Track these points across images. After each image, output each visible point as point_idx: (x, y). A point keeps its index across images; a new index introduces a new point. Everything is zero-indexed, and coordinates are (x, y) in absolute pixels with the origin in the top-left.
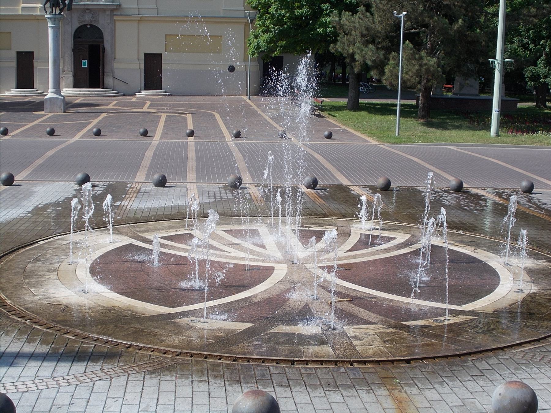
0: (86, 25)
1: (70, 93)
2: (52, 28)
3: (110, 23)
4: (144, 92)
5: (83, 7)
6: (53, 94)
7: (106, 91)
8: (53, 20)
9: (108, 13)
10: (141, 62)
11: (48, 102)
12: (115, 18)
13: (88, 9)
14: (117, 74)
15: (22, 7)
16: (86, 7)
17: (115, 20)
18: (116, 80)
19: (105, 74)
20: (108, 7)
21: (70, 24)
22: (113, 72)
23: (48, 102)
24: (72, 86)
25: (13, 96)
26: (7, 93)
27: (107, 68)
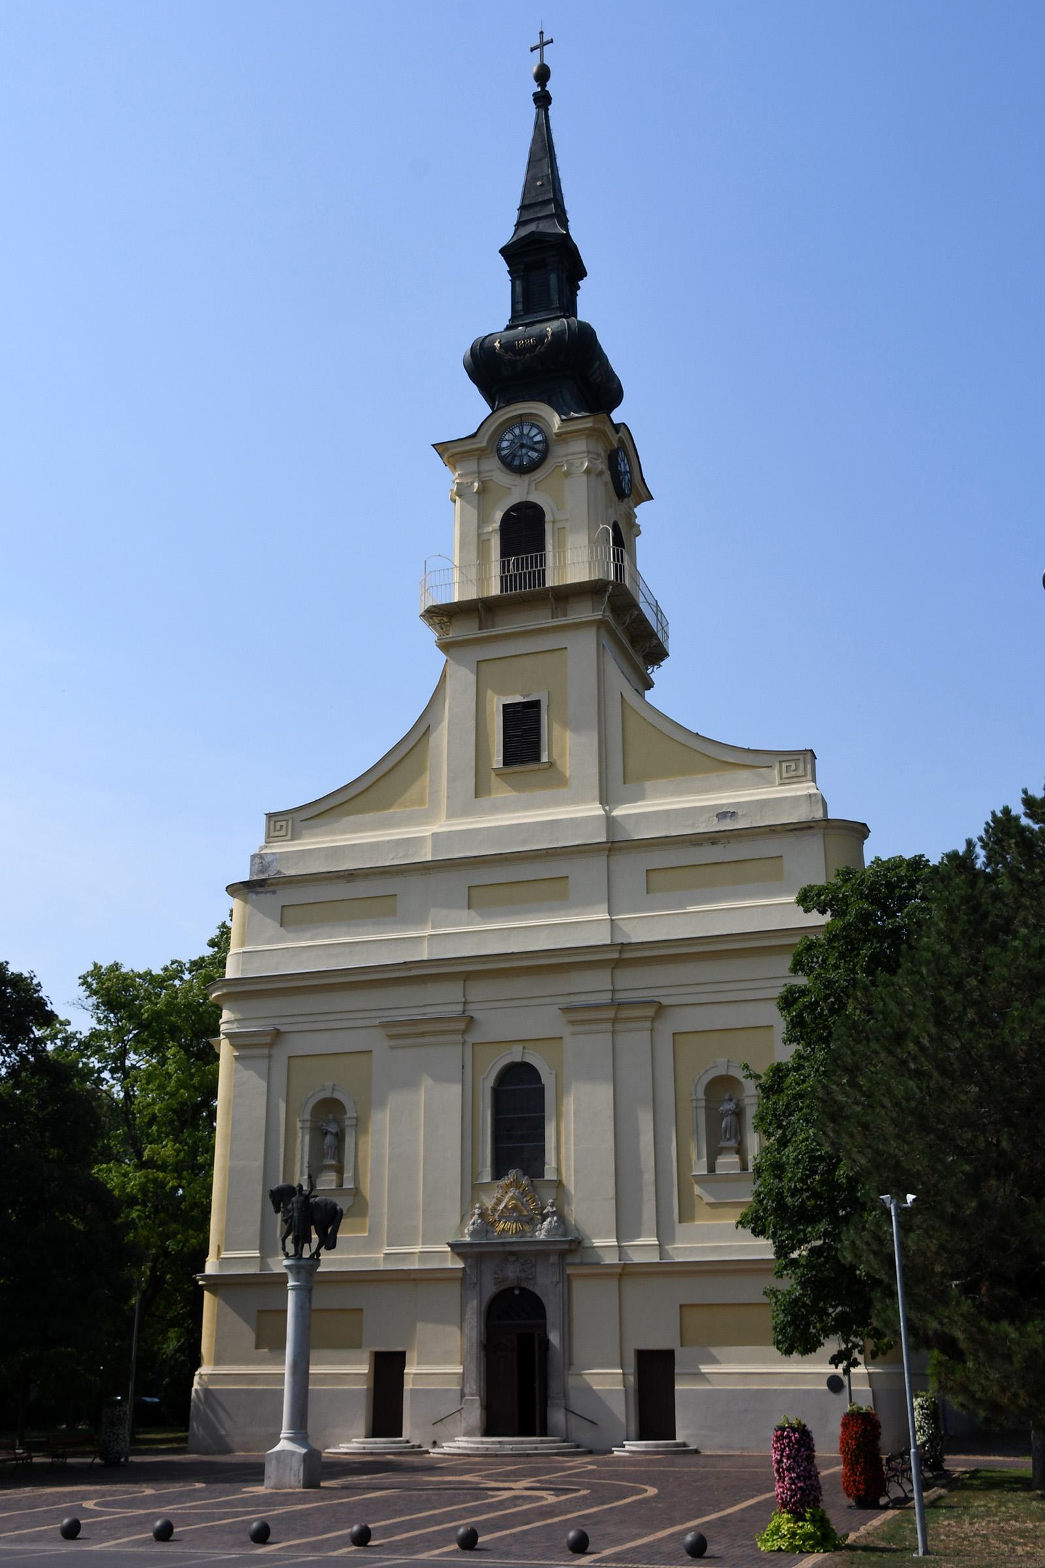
0: (511, 1289)
1: (459, 1448)
2: (294, 1288)
3: (558, 1283)
5: (501, 1249)
7: (542, 1442)
9: (553, 1259)
10: (627, 1371)
11: (274, 1462)
12: (570, 1270)
13: (513, 1253)
14: (576, 1403)
15: (386, 1254)
16: (508, 1248)
17: (569, 1276)
18: (572, 1418)
20: (552, 1247)
22: (566, 1396)
26: (344, 1448)
27: (554, 1387)
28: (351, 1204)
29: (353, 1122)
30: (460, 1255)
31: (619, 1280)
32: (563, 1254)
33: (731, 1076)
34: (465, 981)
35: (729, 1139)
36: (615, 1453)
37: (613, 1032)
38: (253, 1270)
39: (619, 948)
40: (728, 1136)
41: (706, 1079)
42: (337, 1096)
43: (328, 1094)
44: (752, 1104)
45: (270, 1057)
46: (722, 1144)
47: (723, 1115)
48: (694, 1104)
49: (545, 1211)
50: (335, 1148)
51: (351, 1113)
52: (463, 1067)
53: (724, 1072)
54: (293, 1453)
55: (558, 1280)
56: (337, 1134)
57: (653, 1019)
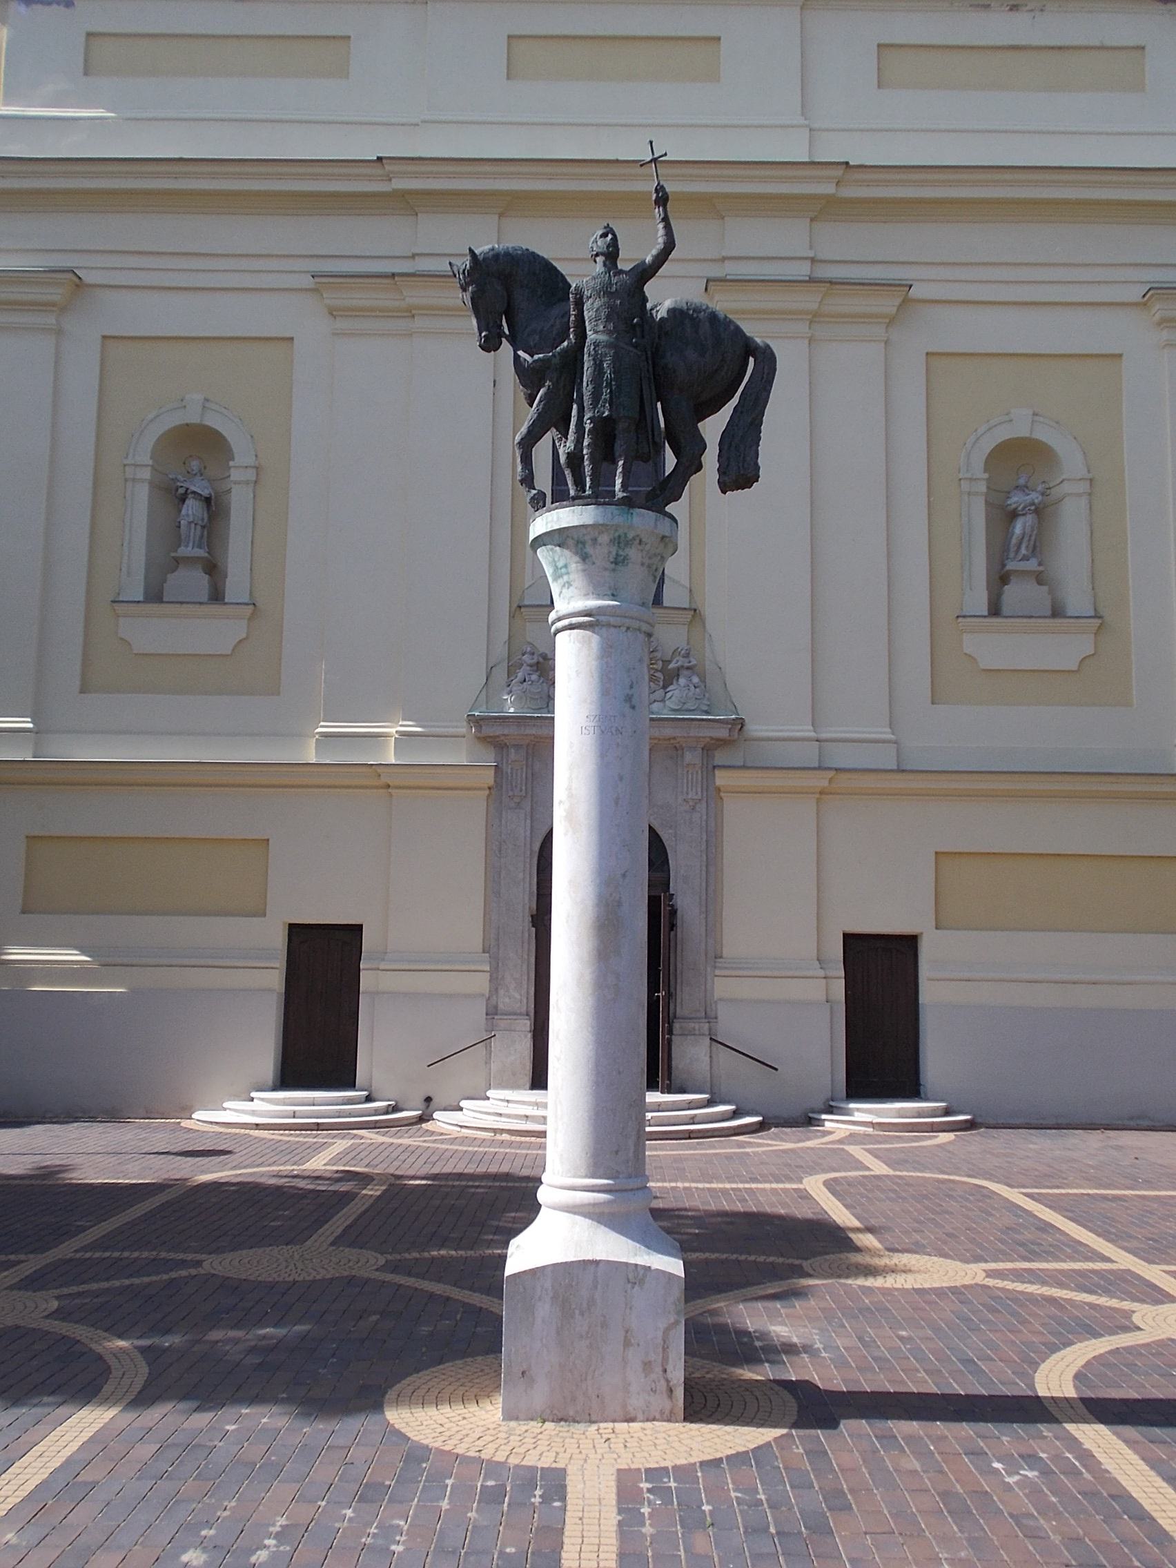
2: (592, 622)
4: (865, 1112)
6: (583, 1223)
8: (602, 551)
11: (544, 1310)
17: (718, 790)
19: (677, 1026)
21: (527, 805)
22: (710, 1018)
23: (544, 1310)
24: (528, 1085)
25: (257, 1126)
26: (234, 1112)
28: (244, 635)
29: (251, 475)
30: (485, 740)
31: (818, 800)
32: (710, 748)
33: (1037, 442)
34: (501, 215)
35: (1025, 558)
36: (827, 1124)
37: (811, 340)
38: (25, 754)
39: (839, 172)
40: (1023, 551)
41: (988, 445)
42: (213, 421)
43: (193, 417)
44: (1079, 495)
45: (59, 332)
46: (1011, 566)
47: (1013, 515)
48: (965, 486)
49: (671, 666)
50: (203, 527)
51: (243, 455)
52: (495, 381)
53: (1023, 432)
54: (637, 1276)
55: (699, 796)
56: (208, 500)
57: (891, 321)
